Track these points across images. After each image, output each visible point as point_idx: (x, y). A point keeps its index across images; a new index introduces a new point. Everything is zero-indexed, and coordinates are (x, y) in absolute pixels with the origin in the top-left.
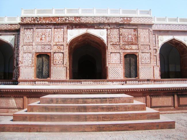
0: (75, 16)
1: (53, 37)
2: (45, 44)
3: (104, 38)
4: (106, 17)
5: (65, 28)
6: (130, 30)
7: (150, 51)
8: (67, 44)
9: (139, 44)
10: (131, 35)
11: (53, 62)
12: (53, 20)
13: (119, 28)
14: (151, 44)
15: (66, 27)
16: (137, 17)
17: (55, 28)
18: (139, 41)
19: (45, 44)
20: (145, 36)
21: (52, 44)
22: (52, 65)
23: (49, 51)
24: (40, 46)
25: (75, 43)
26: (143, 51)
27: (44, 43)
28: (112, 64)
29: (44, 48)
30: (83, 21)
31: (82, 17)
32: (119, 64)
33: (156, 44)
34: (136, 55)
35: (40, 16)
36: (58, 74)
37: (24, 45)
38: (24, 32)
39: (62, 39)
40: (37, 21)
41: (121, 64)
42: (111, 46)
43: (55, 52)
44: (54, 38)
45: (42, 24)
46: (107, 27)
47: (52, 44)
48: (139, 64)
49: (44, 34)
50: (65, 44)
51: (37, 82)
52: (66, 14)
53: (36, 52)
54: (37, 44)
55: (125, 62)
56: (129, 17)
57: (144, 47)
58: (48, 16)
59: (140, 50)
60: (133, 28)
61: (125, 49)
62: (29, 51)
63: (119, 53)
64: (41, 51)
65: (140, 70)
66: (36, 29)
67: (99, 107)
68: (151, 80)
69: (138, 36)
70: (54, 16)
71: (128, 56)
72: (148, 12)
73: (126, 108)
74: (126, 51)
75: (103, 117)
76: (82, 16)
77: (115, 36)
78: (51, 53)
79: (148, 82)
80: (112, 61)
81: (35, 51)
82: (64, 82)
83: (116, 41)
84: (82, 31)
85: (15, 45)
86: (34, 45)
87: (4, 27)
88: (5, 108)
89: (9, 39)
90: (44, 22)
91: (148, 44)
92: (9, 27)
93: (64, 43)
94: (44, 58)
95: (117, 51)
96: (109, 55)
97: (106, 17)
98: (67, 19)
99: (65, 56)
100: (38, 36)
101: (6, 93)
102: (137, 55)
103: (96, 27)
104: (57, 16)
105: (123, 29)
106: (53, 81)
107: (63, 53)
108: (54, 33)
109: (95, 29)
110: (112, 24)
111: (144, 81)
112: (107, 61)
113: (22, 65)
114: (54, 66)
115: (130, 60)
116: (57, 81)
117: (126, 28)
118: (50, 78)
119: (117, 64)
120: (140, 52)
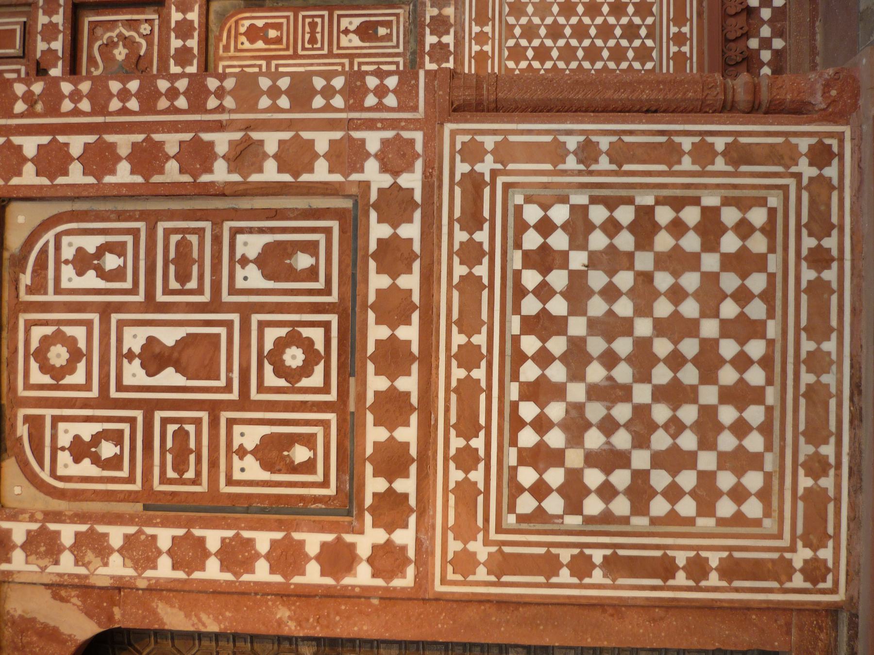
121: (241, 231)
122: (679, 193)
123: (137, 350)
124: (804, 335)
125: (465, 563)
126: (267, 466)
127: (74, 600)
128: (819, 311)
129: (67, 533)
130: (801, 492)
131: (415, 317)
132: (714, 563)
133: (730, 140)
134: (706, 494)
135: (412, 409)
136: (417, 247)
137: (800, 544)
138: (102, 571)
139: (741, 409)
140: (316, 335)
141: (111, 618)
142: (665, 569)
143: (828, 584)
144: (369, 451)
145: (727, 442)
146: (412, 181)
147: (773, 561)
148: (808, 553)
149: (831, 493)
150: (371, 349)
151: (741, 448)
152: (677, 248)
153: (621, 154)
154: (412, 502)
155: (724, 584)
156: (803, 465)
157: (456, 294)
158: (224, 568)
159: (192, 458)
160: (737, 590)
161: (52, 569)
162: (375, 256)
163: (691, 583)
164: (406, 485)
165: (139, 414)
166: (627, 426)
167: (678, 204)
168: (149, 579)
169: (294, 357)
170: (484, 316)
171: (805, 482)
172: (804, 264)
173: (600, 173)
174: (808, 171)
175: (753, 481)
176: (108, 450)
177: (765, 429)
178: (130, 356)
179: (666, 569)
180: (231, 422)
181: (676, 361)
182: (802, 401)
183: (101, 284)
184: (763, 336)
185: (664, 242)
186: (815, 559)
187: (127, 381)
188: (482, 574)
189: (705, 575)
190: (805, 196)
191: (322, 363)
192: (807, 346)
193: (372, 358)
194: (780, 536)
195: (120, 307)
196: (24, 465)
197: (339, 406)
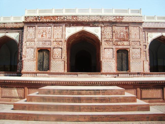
0: (72, 15)
1: (53, 34)
2: (46, 40)
3: (98, 35)
4: (101, 16)
5: (63, 25)
6: (121, 28)
7: (140, 47)
8: (65, 41)
9: (130, 40)
10: (123, 32)
11: (53, 56)
12: (52, 19)
13: (112, 26)
14: (141, 40)
15: (64, 25)
16: (128, 16)
17: (54, 26)
18: (130, 38)
19: (45, 40)
20: (136, 33)
21: (52, 40)
22: (52, 59)
23: (49, 47)
24: (41, 42)
25: (72, 39)
26: (133, 47)
27: (45, 39)
29: (45, 44)
30: (80, 19)
31: (79, 16)
32: (112, 58)
33: (145, 40)
34: (127, 51)
35: (41, 16)
36: (57, 67)
37: (27, 41)
38: (27, 29)
39: (61, 36)
40: (39, 20)
41: (114, 59)
42: (105, 42)
43: (54, 47)
44: (54, 35)
45: (43, 23)
46: (101, 25)
47: (52, 40)
48: (130, 59)
49: (44, 31)
50: (63, 40)
51: (38, 75)
52: (64, 13)
53: (37, 47)
54: (39, 40)
55: (117, 56)
56: (121, 16)
57: (135, 43)
58: (48, 16)
59: (131, 46)
60: (125, 25)
61: (117, 45)
62: (31, 47)
63: (112, 48)
64: (42, 47)
65: (131, 64)
66: (38, 26)
67: (93, 98)
68: (141, 73)
69: (130, 33)
70: (54, 15)
71: (120, 51)
72: (139, 11)
73: (118, 100)
74: (118, 47)
75: (96, 108)
76: (78, 15)
77: (108, 33)
78: (50, 48)
79: (138, 75)
80: (106, 56)
81: (37, 47)
82: (62, 74)
83: (110, 37)
84: (79, 29)
85: (19, 41)
86: (36, 41)
87: (10, 25)
88: (8, 98)
89: (14, 35)
90: (45, 20)
91: (138, 40)
92: (15, 26)
93: (63, 39)
94: (44, 53)
95: (110, 46)
96: (103, 50)
97: (100, 16)
98: (66, 18)
99: (63, 51)
100: (39, 33)
101: (9, 84)
102: (128, 50)
103: (91, 25)
104: (57, 15)
105: (115, 27)
106: (53, 73)
107: (61, 48)
108: (54, 30)
109: (91, 26)
110: (106, 22)
111: (135, 74)
112: (101, 56)
113: (25, 58)
114: (54, 60)
115: (122, 55)
116: (56, 74)
117: (118, 25)
118: (50, 70)
120: (131, 47)
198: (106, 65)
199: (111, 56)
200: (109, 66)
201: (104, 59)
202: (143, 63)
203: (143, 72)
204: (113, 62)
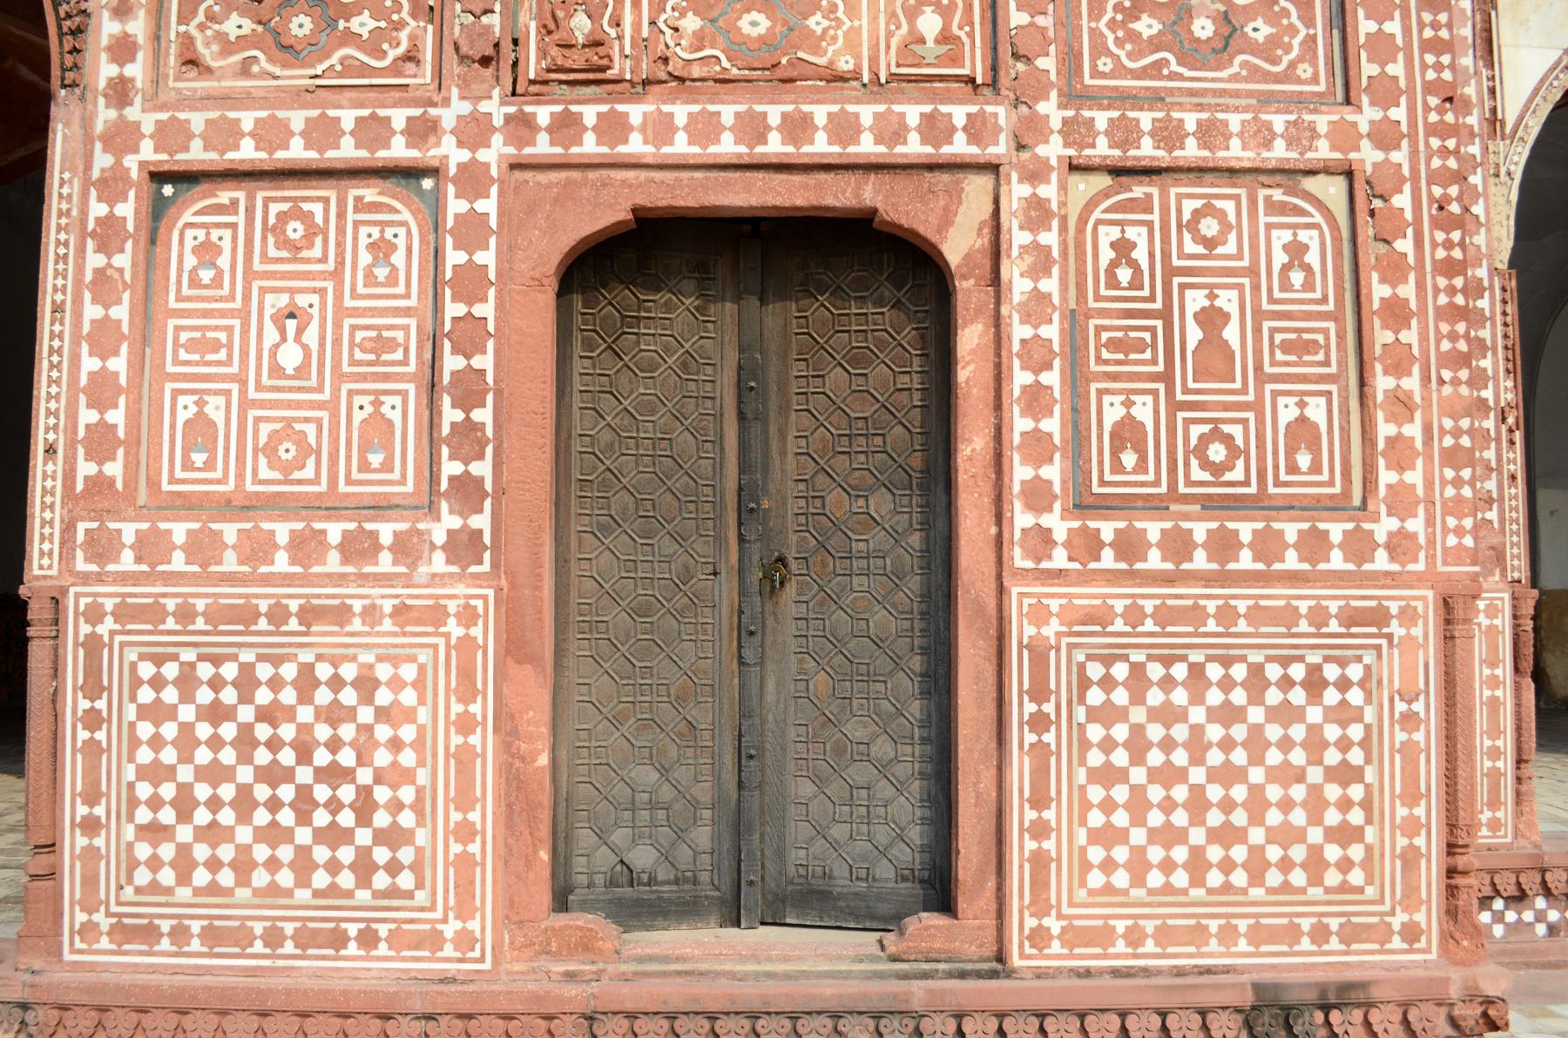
7: (1345, 136)
26: (1124, 133)
28: (185, 505)
32: (381, 508)
48: (1022, 519)
59: (1050, 109)
65: (1021, 708)
80: (200, 428)
102: (958, 247)
119: (332, 508)
121: (1329, 403)
122: (1376, 805)
123: (1217, 303)
124: (1252, 921)
125: (1040, 614)
126: (1119, 426)
127: (979, 242)
128: (1273, 935)
129: (1050, 238)
130: (1111, 922)
131: (1260, 566)
132: (1046, 845)
133: (1423, 850)
134: (1108, 836)
135: (1178, 564)
136: (1322, 566)
137: (1064, 923)
138: (1016, 272)
139: (1185, 866)
140: (1237, 474)
141: (964, 277)
142: (1039, 801)
143: (1028, 950)
144: (1138, 525)
145: (1155, 854)
146: (1381, 561)
147: (1048, 899)
148: (1056, 931)
149: (1111, 950)
150: (1231, 525)
151: (1149, 866)
152: (1327, 804)
153: (1409, 752)
154: (1093, 565)
155: (1027, 855)
156: (1136, 925)
157: (1282, 603)
158: (1024, 388)
159: (1121, 356)
160: (1021, 867)
161: (1015, 224)
162: (1314, 528)
163: (1027, 824)
164: (1108, 560)
165: (1158, 305)
166: (1168, 762)
167: (1366, 805)
168: (1010, 317)
169: (1217, 452)
170: (1263, 630)
171: (1120, 926)
172: (1314, 920)
173: (1392, 733)
174: (1396, 922)
175: (1121, 879)
176: (1124, 275)
177: (1168, 889)
178: (1212, 297)
179: (1039, 802)
180: (1155, 393)
181: (1227, 805)
182: (1193, 922)
183: (1276, 268)
184: (1251, 884)
185: (1333, 792)
186: (1051, 938)
187: (1189, 293)
188: (1029, 631)
189: (1034, 837)
190: (1375, 920)
191: (1211, 479)
192: (1243, 925)
193: (1222, 526)
194: (1071, 904)
195: (1256, 288)
196: (1106, 194)
197: (1173, 495)
198: (186, 742)
199: (379, 428)
200: (273, 775)
201: (129, 531)
202: (1430, 653)
203: (1428, 953)
204: (430, 650)
